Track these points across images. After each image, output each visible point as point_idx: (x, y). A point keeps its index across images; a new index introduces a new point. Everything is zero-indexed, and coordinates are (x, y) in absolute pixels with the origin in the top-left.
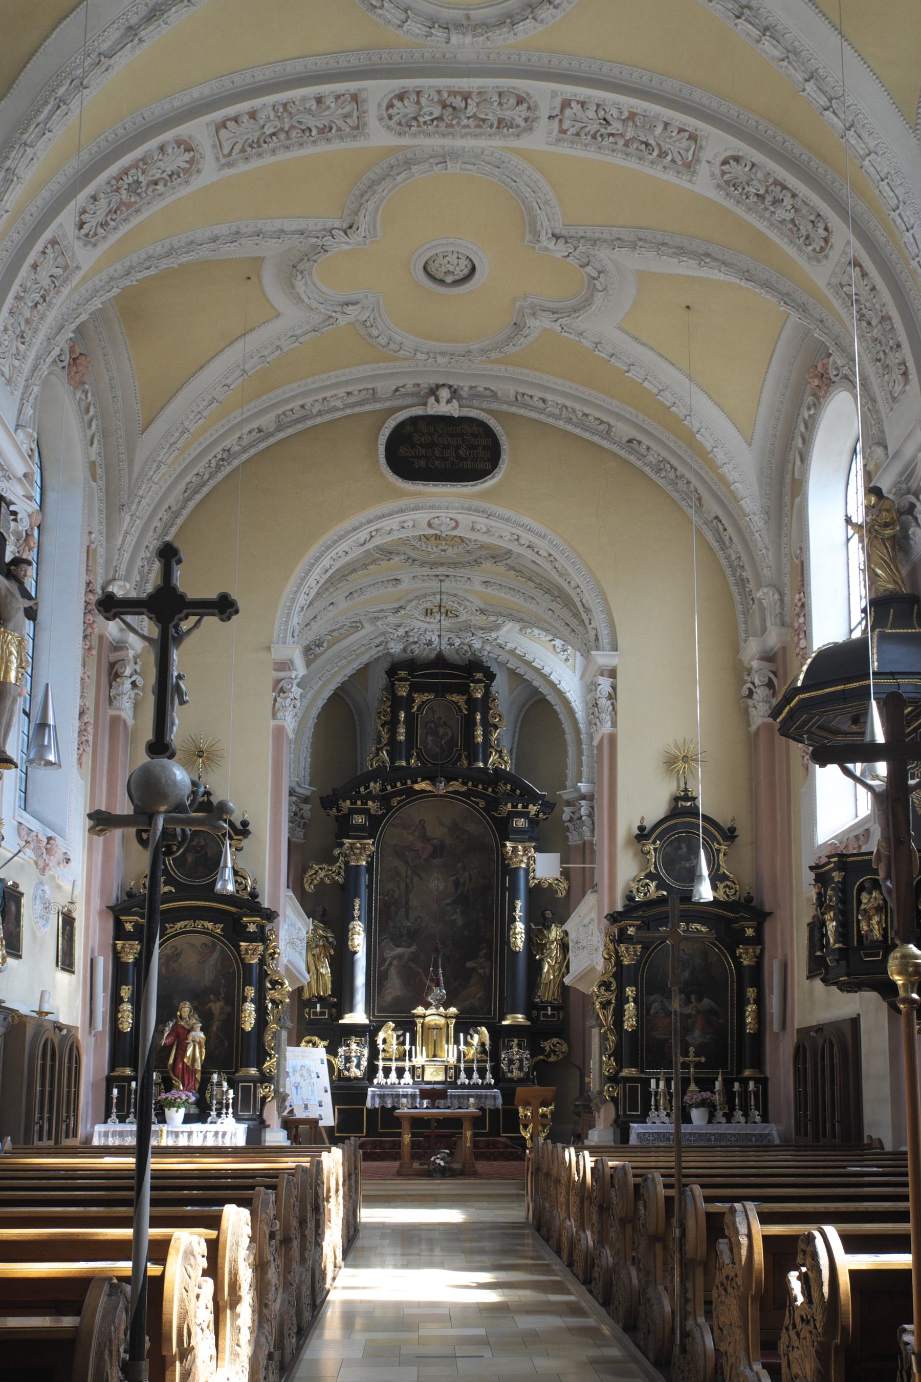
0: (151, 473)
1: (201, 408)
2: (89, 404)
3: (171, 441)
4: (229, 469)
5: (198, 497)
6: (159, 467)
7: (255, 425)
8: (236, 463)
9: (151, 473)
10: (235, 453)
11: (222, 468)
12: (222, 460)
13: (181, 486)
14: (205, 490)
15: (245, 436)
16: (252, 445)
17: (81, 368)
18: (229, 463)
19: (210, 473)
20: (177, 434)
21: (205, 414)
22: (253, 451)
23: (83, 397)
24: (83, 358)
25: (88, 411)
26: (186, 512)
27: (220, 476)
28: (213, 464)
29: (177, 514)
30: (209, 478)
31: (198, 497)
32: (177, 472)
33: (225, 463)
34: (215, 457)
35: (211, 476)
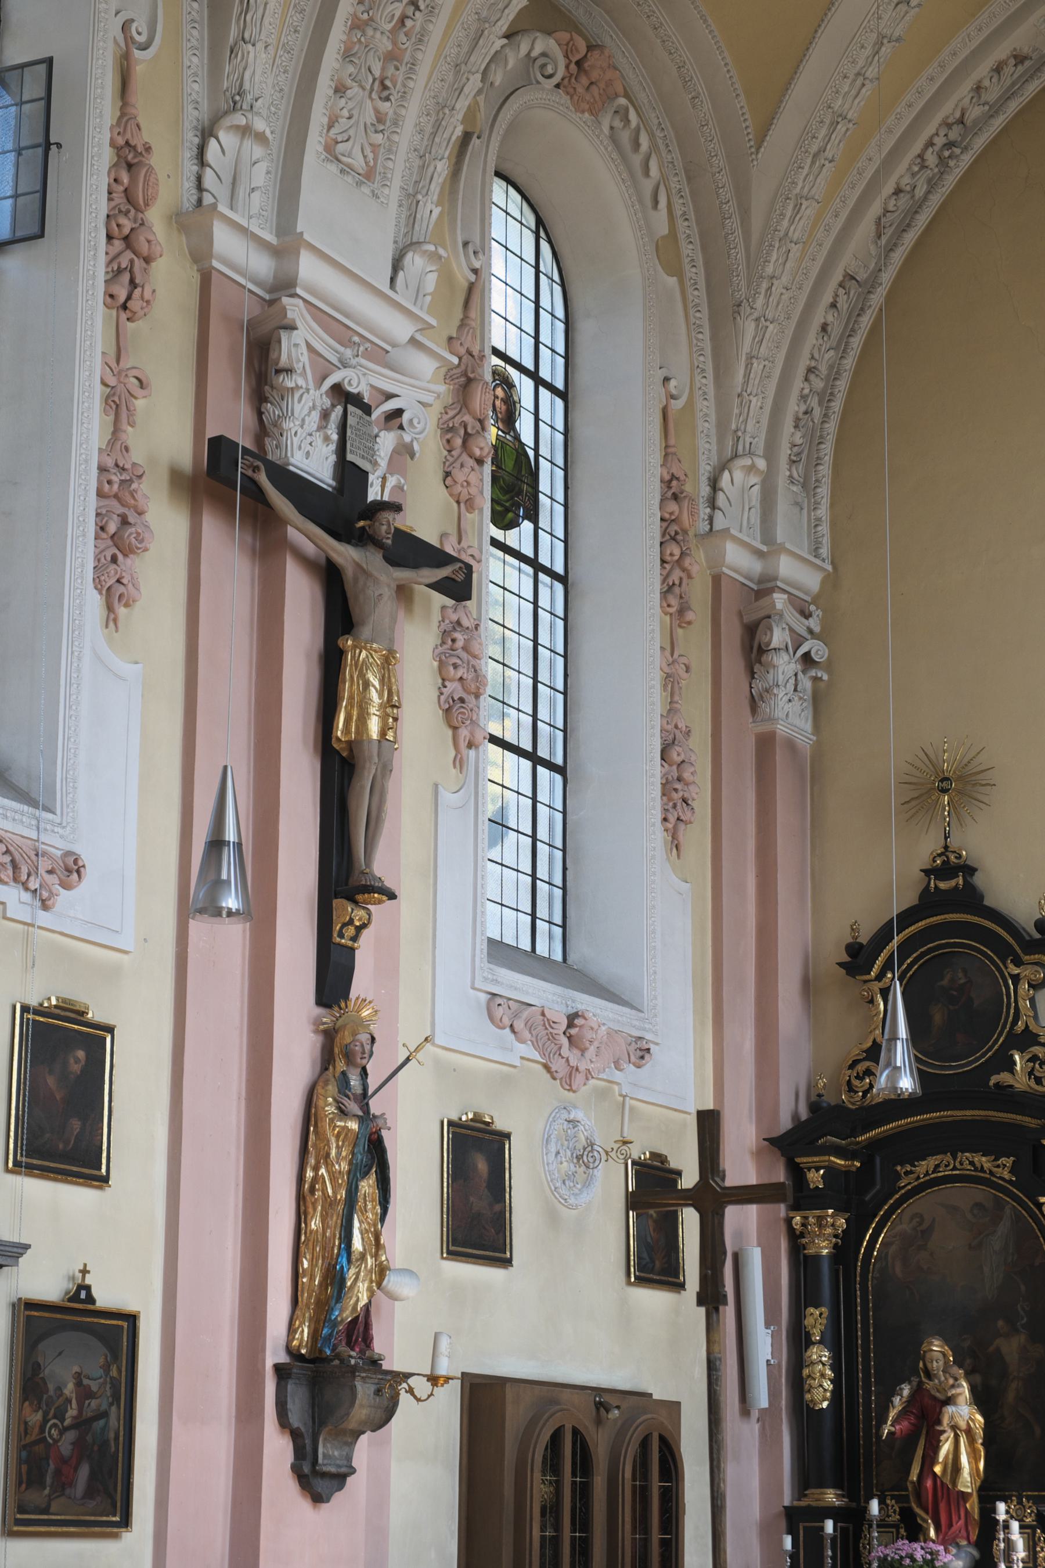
0: (785, 223)
1: (861, 63)
2: (638, 131)
3: (814, 148)
4: (967, 159)
5: (910, 238)
6: (797, 208)
7: (1002, 52)
8: (980, 142)
9: (785, 223)
10: (976, 122)
11: (952, 163)
12: (950, 145)
13: (866, 227)
14: (923, 219)
15: (986, 83)
16: (1008, 96)
17: (595, 75)
18: (965, 149)
19: (929, 181)
20: (823, 132)
21: (871, 73)
22: (1013, 106)
23: (618, 124)
24: (596, 53)
25: (636, 145)
26: (887, 277)
27: (951, 180)
28: (931, 159)
29: (870, 286)
30: (928, 192)
31: (910, 238)
32: (851, 203)
33: (957, 151)
34: (930, 144)
35: (932, 185)
